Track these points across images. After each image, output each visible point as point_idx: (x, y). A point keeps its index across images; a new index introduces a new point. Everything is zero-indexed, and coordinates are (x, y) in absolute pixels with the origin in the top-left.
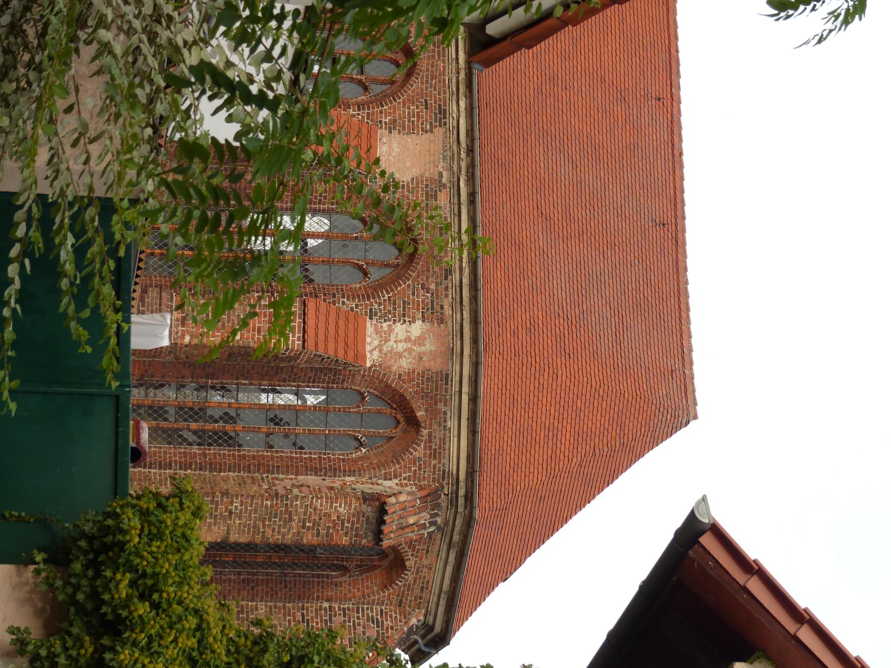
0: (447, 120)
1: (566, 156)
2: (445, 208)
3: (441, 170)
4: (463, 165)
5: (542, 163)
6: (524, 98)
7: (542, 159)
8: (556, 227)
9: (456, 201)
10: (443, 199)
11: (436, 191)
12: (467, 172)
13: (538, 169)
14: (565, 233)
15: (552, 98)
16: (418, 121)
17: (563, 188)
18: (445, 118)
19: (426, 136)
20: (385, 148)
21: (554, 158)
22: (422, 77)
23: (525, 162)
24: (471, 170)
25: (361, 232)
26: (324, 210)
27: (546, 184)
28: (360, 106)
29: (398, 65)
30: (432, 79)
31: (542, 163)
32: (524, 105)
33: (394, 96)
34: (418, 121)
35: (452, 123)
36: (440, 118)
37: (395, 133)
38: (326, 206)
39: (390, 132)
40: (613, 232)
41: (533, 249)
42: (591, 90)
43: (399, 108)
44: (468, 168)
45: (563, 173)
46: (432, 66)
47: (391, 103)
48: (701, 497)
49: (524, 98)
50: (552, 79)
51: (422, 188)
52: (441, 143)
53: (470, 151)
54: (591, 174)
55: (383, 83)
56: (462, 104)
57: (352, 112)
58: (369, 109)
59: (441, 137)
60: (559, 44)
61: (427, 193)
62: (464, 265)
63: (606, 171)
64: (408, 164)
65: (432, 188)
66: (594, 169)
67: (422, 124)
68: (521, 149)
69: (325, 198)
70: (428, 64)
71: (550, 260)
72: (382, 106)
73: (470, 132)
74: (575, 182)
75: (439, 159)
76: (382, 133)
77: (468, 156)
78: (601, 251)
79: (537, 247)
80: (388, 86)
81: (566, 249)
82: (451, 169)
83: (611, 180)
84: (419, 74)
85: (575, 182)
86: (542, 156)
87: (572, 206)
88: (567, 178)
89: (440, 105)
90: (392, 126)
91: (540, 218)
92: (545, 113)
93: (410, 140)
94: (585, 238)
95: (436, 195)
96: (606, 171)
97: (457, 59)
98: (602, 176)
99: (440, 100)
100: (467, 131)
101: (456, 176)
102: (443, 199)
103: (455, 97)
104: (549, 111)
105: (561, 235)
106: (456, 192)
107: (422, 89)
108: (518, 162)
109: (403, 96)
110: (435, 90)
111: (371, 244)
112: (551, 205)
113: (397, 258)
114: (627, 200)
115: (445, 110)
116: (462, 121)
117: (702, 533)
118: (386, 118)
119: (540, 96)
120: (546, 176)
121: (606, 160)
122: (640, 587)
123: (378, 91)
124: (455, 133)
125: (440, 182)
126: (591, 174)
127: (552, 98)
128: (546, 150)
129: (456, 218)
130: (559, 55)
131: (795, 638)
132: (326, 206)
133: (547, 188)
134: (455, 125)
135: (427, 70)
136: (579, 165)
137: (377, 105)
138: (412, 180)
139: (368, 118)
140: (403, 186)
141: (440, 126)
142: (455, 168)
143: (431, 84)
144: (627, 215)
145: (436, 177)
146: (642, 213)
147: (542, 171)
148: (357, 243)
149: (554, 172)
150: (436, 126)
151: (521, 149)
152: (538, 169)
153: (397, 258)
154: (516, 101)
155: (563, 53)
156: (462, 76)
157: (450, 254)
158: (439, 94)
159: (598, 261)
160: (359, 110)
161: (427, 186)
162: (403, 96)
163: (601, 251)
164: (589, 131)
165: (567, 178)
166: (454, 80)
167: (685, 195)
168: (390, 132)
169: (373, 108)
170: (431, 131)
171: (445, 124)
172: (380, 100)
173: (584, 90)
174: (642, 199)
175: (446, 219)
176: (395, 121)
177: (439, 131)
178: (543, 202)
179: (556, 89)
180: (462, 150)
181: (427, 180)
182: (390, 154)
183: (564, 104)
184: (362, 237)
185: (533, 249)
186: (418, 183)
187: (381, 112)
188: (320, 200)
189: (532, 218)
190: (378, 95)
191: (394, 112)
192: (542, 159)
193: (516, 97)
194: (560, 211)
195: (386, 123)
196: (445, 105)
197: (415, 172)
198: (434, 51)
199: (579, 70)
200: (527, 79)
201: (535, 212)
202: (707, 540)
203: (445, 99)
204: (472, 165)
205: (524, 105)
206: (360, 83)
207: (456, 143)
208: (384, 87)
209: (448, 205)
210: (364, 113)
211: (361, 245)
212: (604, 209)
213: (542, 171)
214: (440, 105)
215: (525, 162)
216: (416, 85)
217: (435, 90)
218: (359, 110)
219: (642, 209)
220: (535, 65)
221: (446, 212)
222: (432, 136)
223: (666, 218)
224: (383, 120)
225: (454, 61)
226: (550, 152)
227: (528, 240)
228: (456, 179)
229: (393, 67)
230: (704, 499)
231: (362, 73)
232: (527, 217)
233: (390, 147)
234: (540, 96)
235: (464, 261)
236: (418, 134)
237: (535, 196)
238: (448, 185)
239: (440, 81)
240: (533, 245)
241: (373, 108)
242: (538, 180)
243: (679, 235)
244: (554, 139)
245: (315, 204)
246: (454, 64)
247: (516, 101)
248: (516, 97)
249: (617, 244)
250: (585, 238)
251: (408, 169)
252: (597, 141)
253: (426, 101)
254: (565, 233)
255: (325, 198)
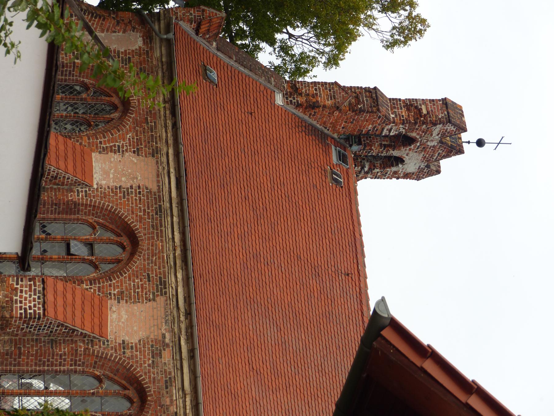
0: (167, 290)
1: (271, 320)
2: (169, 364)
3: (164, 332)
4: (183, 326)
5: (251, 326)
6: (232, 272)
7: (251, 322)
8: (266, 380)
9: (178, 358)
10: (167, 356)
11: (160, 350)
12: (187, 332)
13: (248, 331)
14: (274, 386)
15: (256, 272)
16: (142, 292)
17: (270, 347)
18: (165, 288)
19: (149, 304)
20: (114, 316)
21: (261, 322)
22: (144, 255)
23: (236, 325)
24: (189, 331)
25: (97, 388)
26: (64, 371)
27: (255, 344)
28: (92, 281)
29: (124, 248)
30: (153, 256)
31: (251, 326)
32: (233, 278)
33: (121, 272)
34: (142, 292)
35: (171, 292)
36: (161, 288)
37: (123, 302)
38: (66, 368)
39: (119, 302)
40: (315, 385)
41: (247, 399)
42: (289, 266)
43: (125, 281)
44: (187, 329)
45: (269, 335)
46: (152, 246)
47: (119, 278)
48: (381, 298)
49: (232, 272)
50: (255, 256)
51: (149, 348)
52: (163, 309)
53: (188, 314)
54: (293, 336)
55: (111, 262)
56: (179, 276)
57: (85, 286)
58: (99, 283)
59: (163, 305)
60: (259, 227)
61: (153, 352)
62: (188, 411)
63: (306, 334)
64: (135, 328)
65: (156, 348)
66: (296, 332)
67: (146, 294)
68: (232, 313)
69: (65, 360)
70: (148, 244)
71: (262, 408)
72: (111, 281)
73: (188, 299)
74: (280, 343)
75: (162, 323)
76: (112, 303)
77: (186, 318)
78: (306, 401)
79: (251, 397)
80: (115, 264)
81: (275, 399)
82: (173, 330)
83: (311, 341)
84: (141, 253)
85: (280, 343)
86: (250, 320)
87: (278, 363)
88: (273, 339)
89: (160, 278)
90: (120, 297)
91: (251, 373)
92: (251, 284)
93: (136, 308)
94: (292, 390)
95: (160, 353)
96: (306, 334)
97: (173, 238)
98: (303, 338)
99: (160, 273)
100: (185, 298)
101: (177, 336)
102: (167, 356)
103: (173, 270)
104: (254, 283)
105: (271, 387)
106: (178, 350)
107: (144, 265)
108: (230, 325)
109: (128, 271)
110: (156, 265)
111: (106, 398)
112: (261, 362)
113: (129, 409)
114: (326, 359)
115: (165, 282)
116: (180, 290)
117: (383, 328)
118: (114, 290)
119: (246, 271)
120: (255, 338)
121: (305, 325)
122: (337, 405)
123: (107, 269)
124: (174, 300)
125: (164, 342)
126: (293, 336)
127: (256, 272)
128: (254, 315)
129: (179, 372)
130: (261, 237)
131: (467, 405)
132: (66, 368)
133: (256, 347)
134: (174, 293)
135: (148, 249)
136: (282, 329)
137: (106, 280)
138: (140, 341)
139: (99, 291)
140: (132, 347)
141: (162, 295)
142: (176, 330)
143: (152, 260)
144: (327, 371)
145: (160, 338)
146: (340, 369)
147: (251, 333)
148: (94, 398)
149: (262, 334)
150: (158, 295)
151: (232, 313)
152: (248, 331)
153: (129, 409)
154: (226, 274)
155: (264, 235)
156: (178, 252)
157: (175, 402)
158: (159, 268)
159: (304, 410)
160: (91, 284)
161: (152, 346)
162: (128, 271)
163: (306, 401)
164: (290, 300)
165: (273, 339)
166: (171, 256)
167: (368, 280)
168: (119, 302)
169: (103, 282)
170: (154, 300)
171: (166, 293)
172: (109, 276)
173: (283, 265)
174: (338, 358)
175: (170, 373)
176: (122, 293)
177: (161, 300)
178: (253, 358)
179: (259, 265)
180: (181, 314)
181: (152, 341)
182: (119, 321)
183: (267, 277)
184: (98, 392)
185: (247, 399)
186: (144, 344)
187: (110, 286)
188: (60, 362)
189: (244, 372)
190: (107, 272)
191: (122, 285)
192: (251, 322)
193: (225, 271)
194: (269, 367)
195: (114, 295)
196: (165, 278)
197: (142, 334)
198: (153, 233)
199: (278, 249)
200: (234, 256)
201: (247, 367)
202: (387, 333)
203: (164, 272)
204: (190, 326)
205: (233, 278)
206: (91, 263)
207: (175, 309)
208: (111, 266)
209: (172, 362)
210: (96, 287)
211: (98, 399)
212: (306, 366)
213: (251, 333)
214: (160, 278)
215: (236, 325)
216: (139, 262)
217: (156, 265)
218: (91, 284)
219: (339, 366)
220: (240, 244)
221: (170, 367)
222: (155, 303)
223: (349, 269)
224: (112, 292)
225: (171, 240)
226: (257, 317)
227: (242, 391)
228: (177, 339)
229: (120, 250)
230: (383, 299)
231: (92, 255)
232: (241, 371)
233: (119, 314)
234: (246, 271)
235: (188, 407)
236: (143, 302)
237: (246, 354)
238: (171, 344)
239: (159, 258)
240: (247, 395)
241: (103, 282)
242: (248, 340)
243: (363, 291)
244: (260, 306)
245: (56, 366)
246: (171, 243)
247: (226, 274)
248: (225, 271)
249: (320, 396)
250: (292, 390)
251: (136, 332)
252: (297, 309)
253: (148, 275)
254: (274, 386)
255: (65, 360)
